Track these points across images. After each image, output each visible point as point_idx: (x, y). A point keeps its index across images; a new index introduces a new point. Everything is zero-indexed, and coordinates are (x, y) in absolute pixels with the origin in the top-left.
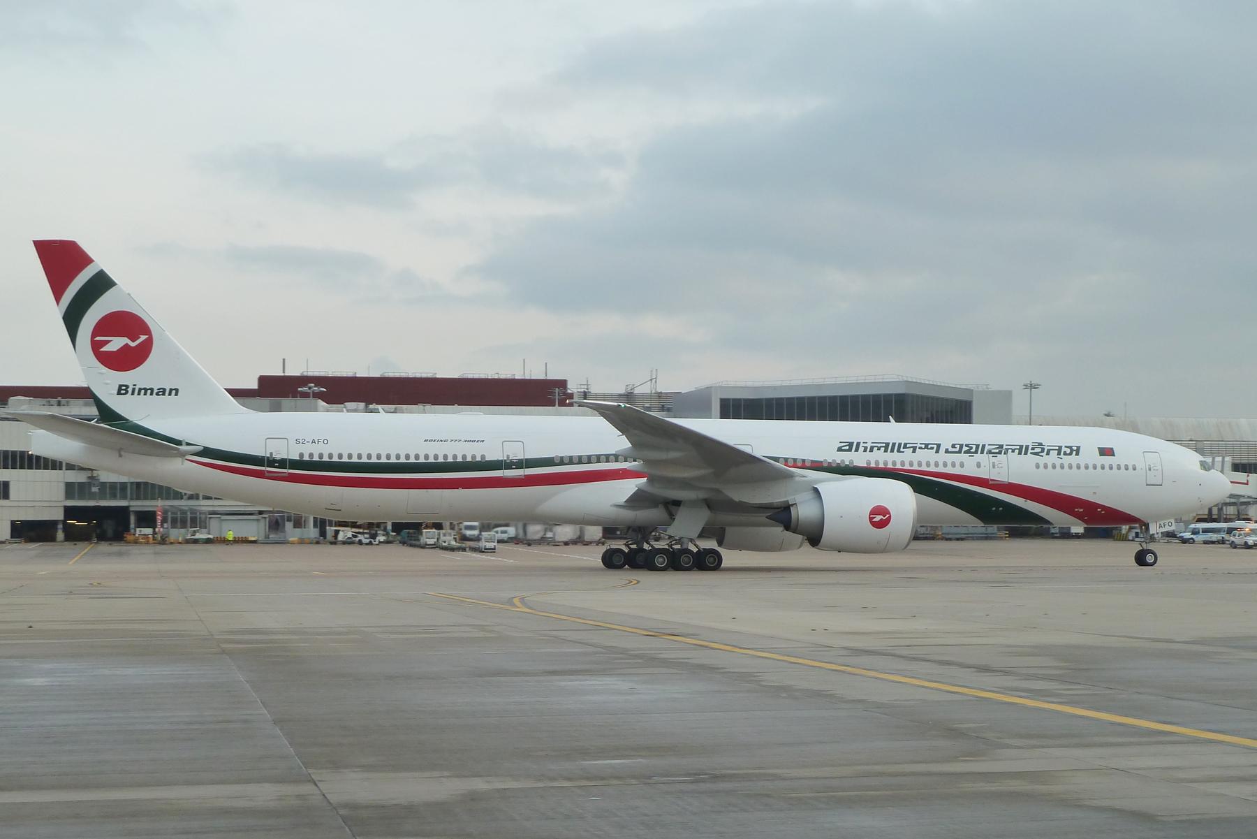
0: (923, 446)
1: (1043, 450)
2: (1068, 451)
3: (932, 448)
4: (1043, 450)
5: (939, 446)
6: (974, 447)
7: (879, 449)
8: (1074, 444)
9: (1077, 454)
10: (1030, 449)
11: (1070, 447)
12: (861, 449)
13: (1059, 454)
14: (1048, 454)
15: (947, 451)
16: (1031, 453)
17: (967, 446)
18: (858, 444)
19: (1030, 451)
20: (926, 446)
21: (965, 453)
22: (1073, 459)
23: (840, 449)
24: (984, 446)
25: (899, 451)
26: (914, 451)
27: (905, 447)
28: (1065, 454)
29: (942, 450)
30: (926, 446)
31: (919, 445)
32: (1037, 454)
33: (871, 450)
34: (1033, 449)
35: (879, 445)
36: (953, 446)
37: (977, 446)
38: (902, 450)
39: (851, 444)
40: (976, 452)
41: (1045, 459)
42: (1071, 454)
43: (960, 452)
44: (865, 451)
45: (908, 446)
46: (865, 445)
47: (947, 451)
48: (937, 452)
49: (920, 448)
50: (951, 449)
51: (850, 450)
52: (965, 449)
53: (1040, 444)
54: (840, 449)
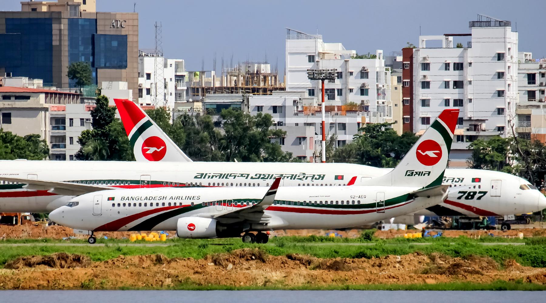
0: (240, 175)
1: (304, 177)
2: (318, 177)
3: (245, 176)
4: (304, 177)
5: (248, 175)
6: (267, 176)
7: (216, 177)
8: (322, 174)
9: (322, 179)
10: (297, 176)
11: (320, 176)
12: (207, 177)
13: (312, 179)
14: (306, 179)
15: (252, 178)
16: (297, 179)
17: (264, 175)
18: (206, 174)
19: (297, 177)
20: (242, 175)
21: (262, 178)
22: (320, 182)
23: (196, 177)
24: (272, 175)
25: (226, 178)
26: (234, 178)
27: (230, 176)
28: (316, 179)
29: (250, 177)
30: (242, 175)
31: (237, 175)
32: (300, 179)
33: (213, 176)
34: (299, 176)
35: (217, 175)
36: (256, 175)
37: (269, 175)
38: (228, 177)
39: (202, 174)
40: (267, 178)
41: (305, 181)
42: (318, 179)
43: (258, 178)
44: (209, 178)
45: (232, 175)
46: (209, 175)
47: (252, 178)
48: (247, 178)
49: (238, 176)
50: (254, 177)
51: (201, 178)
52: (262, 176)
53: (304, 174)
54: (196, 177)
